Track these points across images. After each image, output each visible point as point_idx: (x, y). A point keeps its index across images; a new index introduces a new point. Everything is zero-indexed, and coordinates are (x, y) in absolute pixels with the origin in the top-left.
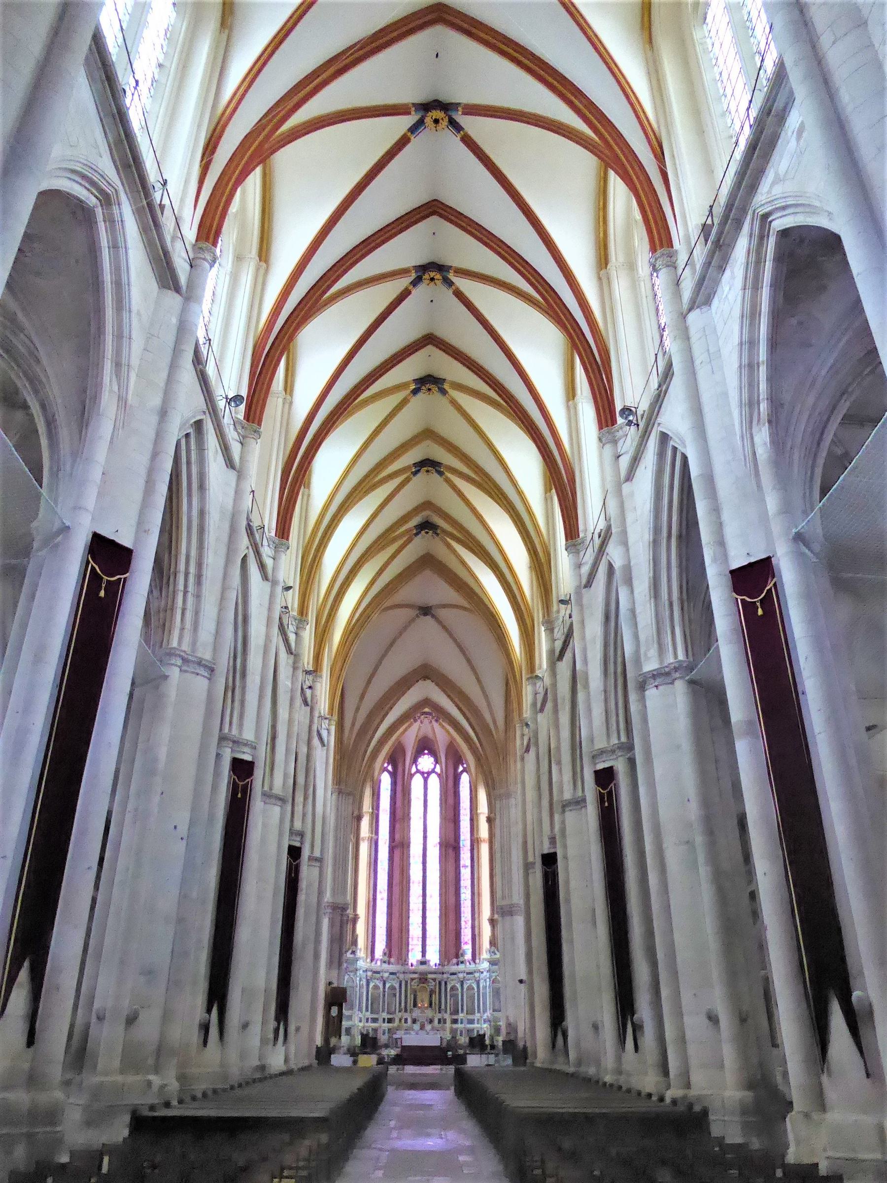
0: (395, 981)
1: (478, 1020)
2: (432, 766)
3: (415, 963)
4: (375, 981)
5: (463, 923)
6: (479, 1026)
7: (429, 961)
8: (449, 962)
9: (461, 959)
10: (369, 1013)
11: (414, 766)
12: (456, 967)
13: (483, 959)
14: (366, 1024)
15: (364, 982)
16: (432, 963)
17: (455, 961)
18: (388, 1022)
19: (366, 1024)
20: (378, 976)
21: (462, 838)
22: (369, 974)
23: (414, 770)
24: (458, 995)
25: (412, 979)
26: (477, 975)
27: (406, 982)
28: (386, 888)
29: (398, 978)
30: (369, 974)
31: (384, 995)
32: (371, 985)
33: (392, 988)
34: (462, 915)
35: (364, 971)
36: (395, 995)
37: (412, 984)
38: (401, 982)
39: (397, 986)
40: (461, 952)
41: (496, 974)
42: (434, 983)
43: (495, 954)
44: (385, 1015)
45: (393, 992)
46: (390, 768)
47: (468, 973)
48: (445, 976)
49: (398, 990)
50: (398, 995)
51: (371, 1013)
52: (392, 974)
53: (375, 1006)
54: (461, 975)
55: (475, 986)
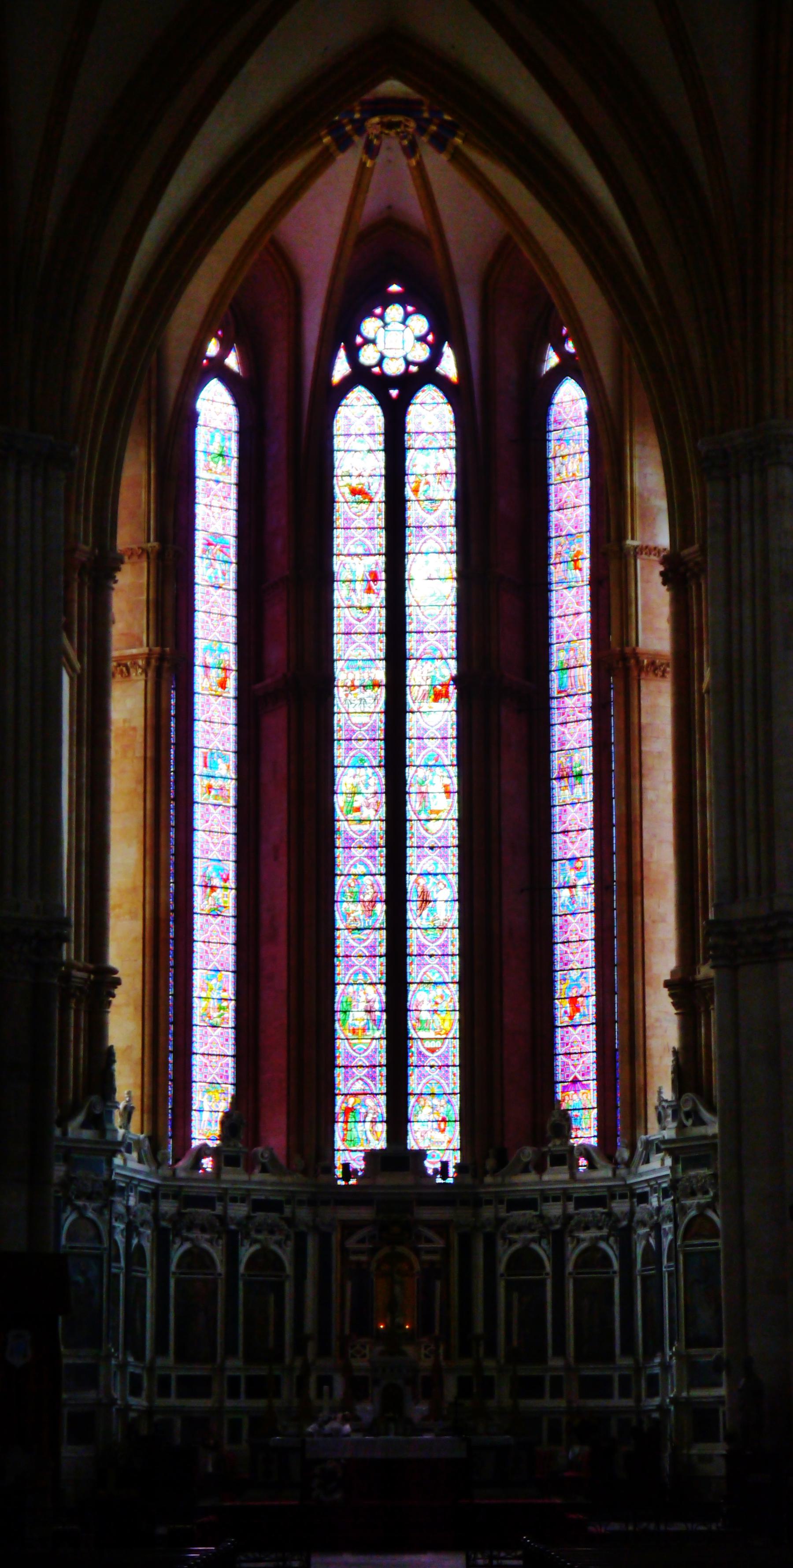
0: (277, 1237)
1: (625, 1381)
2: (422, 353)
3: (358, 1164)
4: (195, 1234)
5: (562, 1008)
6: (629, 1402)
7: (421, 1154)
8: (502, 1160)
9: (555, 1145)
10: (170, 1360)
11: (342, 353)
12: (532, 1177)
13: (648, 1144)
14: (160, 1402)
15: (146, 1240)
16: (431, 1165)
17: (528, 1153)
18: (250, 1395)
19: (160, 1402)
21: (558, 657)
22: (168, 1207)
23: (341, 368)
24: (543, 1283)
25: (349, 1228)
26: (620, 1207)
28: (231, 867)
30: (168, 1207)
32: (178, 1252)
34: (558, 975)
35: (144, 1197)
36: (278, 1289)
37: (351, 1243)
39: (286, 1255)
40: (555, 1118)
41: (701, 1199)
42: (439, 1243)
43: (700, 1122)
44: (235, 1365)
46: (232, 361)
47: (582, 1202)
48: (487, 1213)
49: (289, 1269)
51: (181, 1356)
52: (258, 1205)
54: (554, 1210)
55: (610, 1250)
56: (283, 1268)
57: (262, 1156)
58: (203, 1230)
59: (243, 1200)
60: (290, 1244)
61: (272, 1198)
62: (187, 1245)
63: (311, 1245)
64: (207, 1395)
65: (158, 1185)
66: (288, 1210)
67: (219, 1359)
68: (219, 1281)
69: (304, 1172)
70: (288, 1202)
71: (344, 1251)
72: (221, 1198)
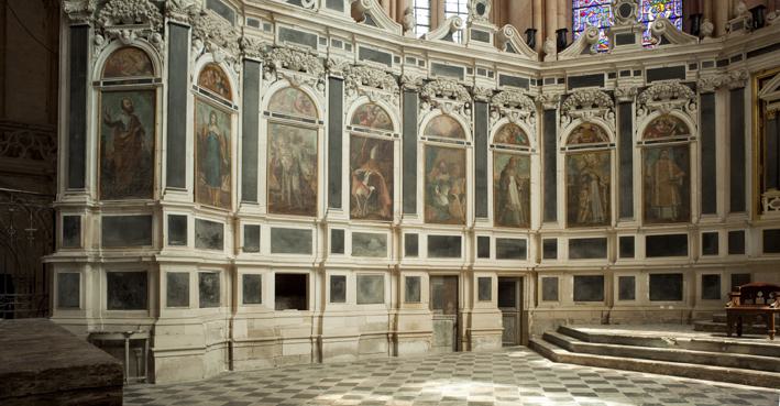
20: (590, 92)
22: (554, 90)
27: (737, 94)
29: (693, 86)
30: (554, 90)
31: (626, 162)
33: (667, 128)
36: (684, 150)
38: (707, 102)
39: (692, 119)
45: (673, 141)
49: (695, 132)
50: (695, 151)
51: (572, 220)
52: (654, 75)
53: (591, 195)
56: (687, 131)
57: (657, 28)
58: (594, 106)
59: (637, 73)
60: (695, 111)
61: (670, 66)
62: (577, 123)
63: (721, 106)
64: (604, 256)
65: (538, 72)
66: (690, 76)
67: (613, 223)
68: (613, 151)
69: (714, 34)
70: (693, 67)
71: (761, 103)
72: (612, 76)
